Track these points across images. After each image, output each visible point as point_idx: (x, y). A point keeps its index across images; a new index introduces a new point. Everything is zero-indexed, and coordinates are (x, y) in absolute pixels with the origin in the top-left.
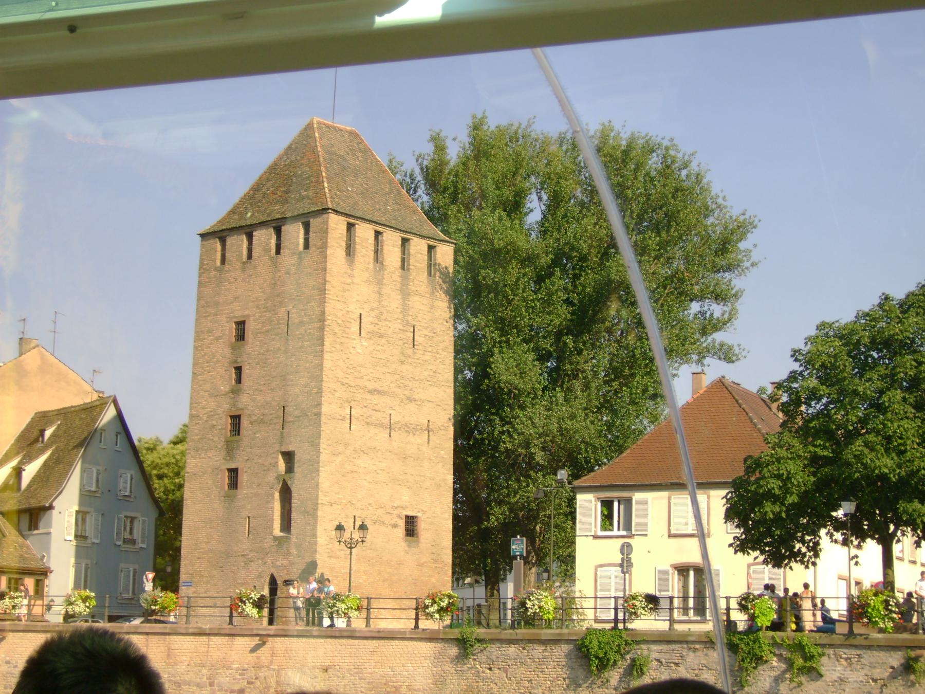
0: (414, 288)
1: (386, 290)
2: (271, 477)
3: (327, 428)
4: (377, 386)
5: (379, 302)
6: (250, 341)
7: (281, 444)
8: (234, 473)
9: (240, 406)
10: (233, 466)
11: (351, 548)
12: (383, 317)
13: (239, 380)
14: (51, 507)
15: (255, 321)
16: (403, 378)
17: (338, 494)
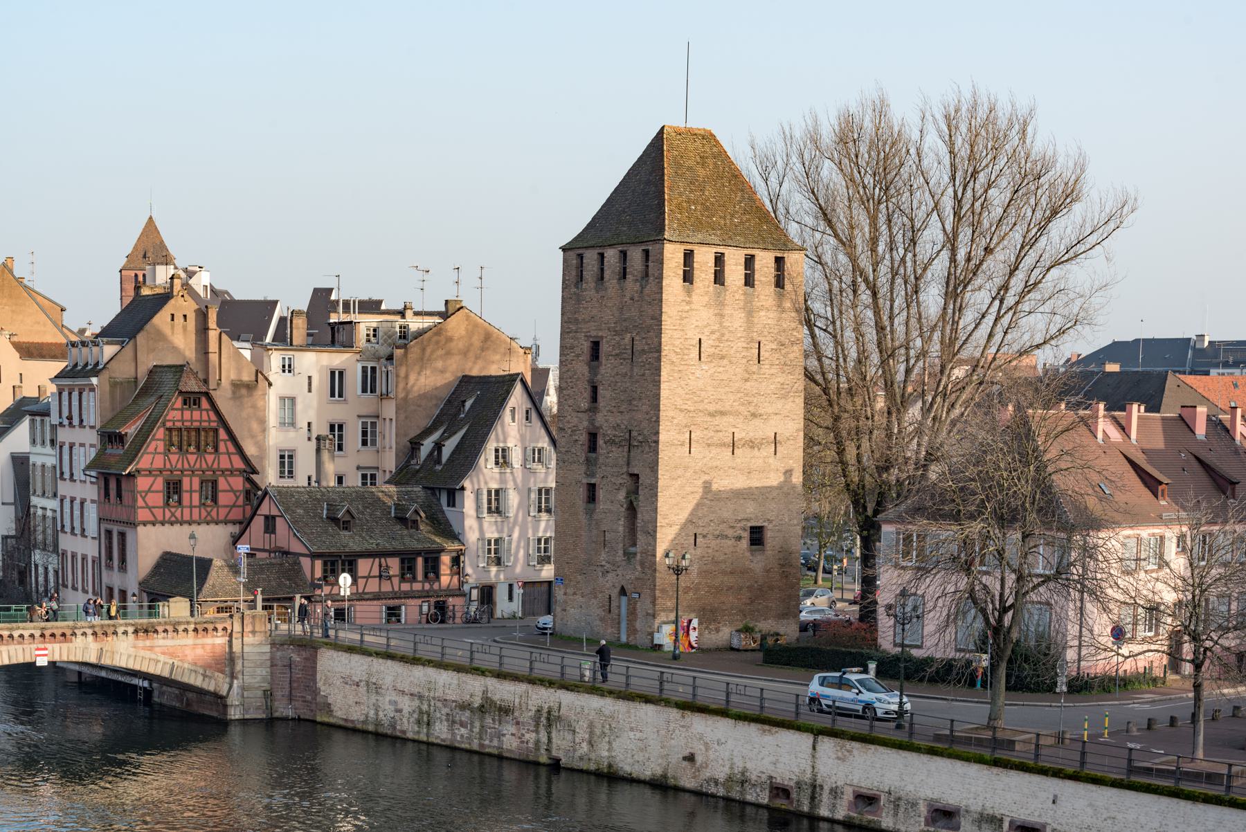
0: (759, 304)
1: (728, 311)
2: (621, 495)
3: (665, 455)
4: (719, 407)
5: (721, 324)
6: (604, 362)
7: (628, 464)
8: (592, 488)
9: (597, 424)
10: (593, 481)
11: (678, 575)
12: (725, 338)
13: (594, 399)
14: (463, 489)
15: (607, 342)
16: (747, 395)
17: (678, 515)
